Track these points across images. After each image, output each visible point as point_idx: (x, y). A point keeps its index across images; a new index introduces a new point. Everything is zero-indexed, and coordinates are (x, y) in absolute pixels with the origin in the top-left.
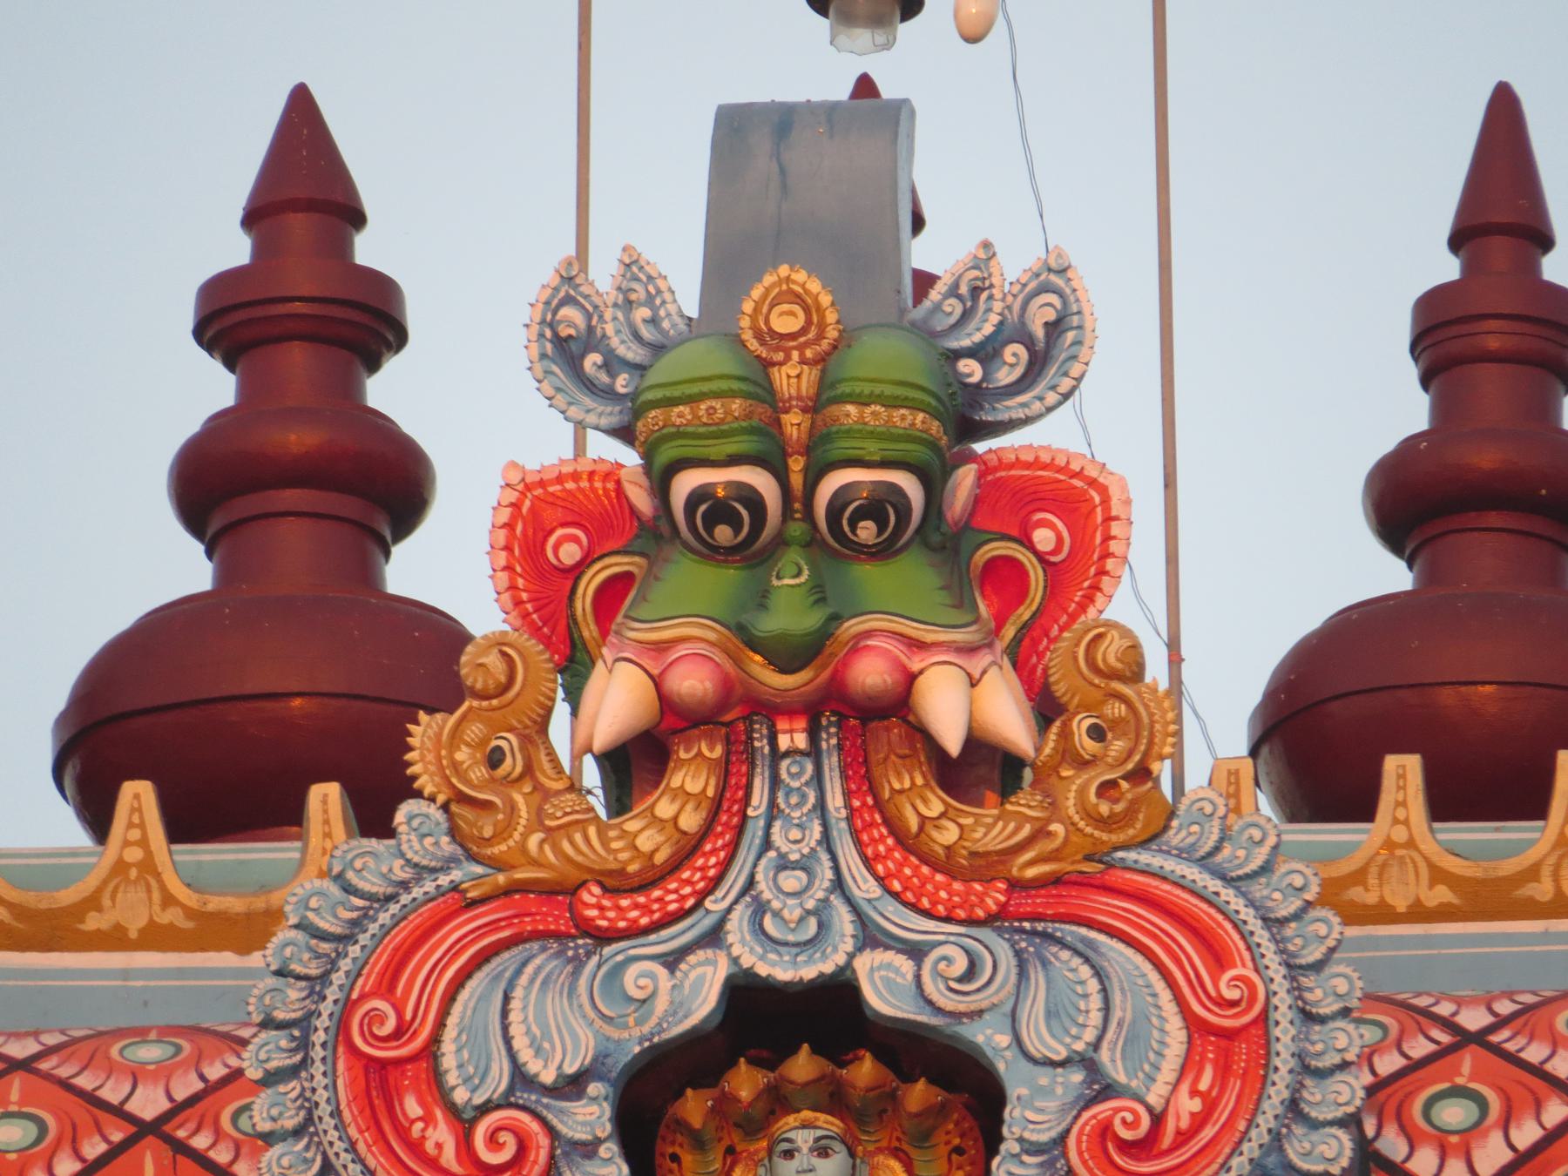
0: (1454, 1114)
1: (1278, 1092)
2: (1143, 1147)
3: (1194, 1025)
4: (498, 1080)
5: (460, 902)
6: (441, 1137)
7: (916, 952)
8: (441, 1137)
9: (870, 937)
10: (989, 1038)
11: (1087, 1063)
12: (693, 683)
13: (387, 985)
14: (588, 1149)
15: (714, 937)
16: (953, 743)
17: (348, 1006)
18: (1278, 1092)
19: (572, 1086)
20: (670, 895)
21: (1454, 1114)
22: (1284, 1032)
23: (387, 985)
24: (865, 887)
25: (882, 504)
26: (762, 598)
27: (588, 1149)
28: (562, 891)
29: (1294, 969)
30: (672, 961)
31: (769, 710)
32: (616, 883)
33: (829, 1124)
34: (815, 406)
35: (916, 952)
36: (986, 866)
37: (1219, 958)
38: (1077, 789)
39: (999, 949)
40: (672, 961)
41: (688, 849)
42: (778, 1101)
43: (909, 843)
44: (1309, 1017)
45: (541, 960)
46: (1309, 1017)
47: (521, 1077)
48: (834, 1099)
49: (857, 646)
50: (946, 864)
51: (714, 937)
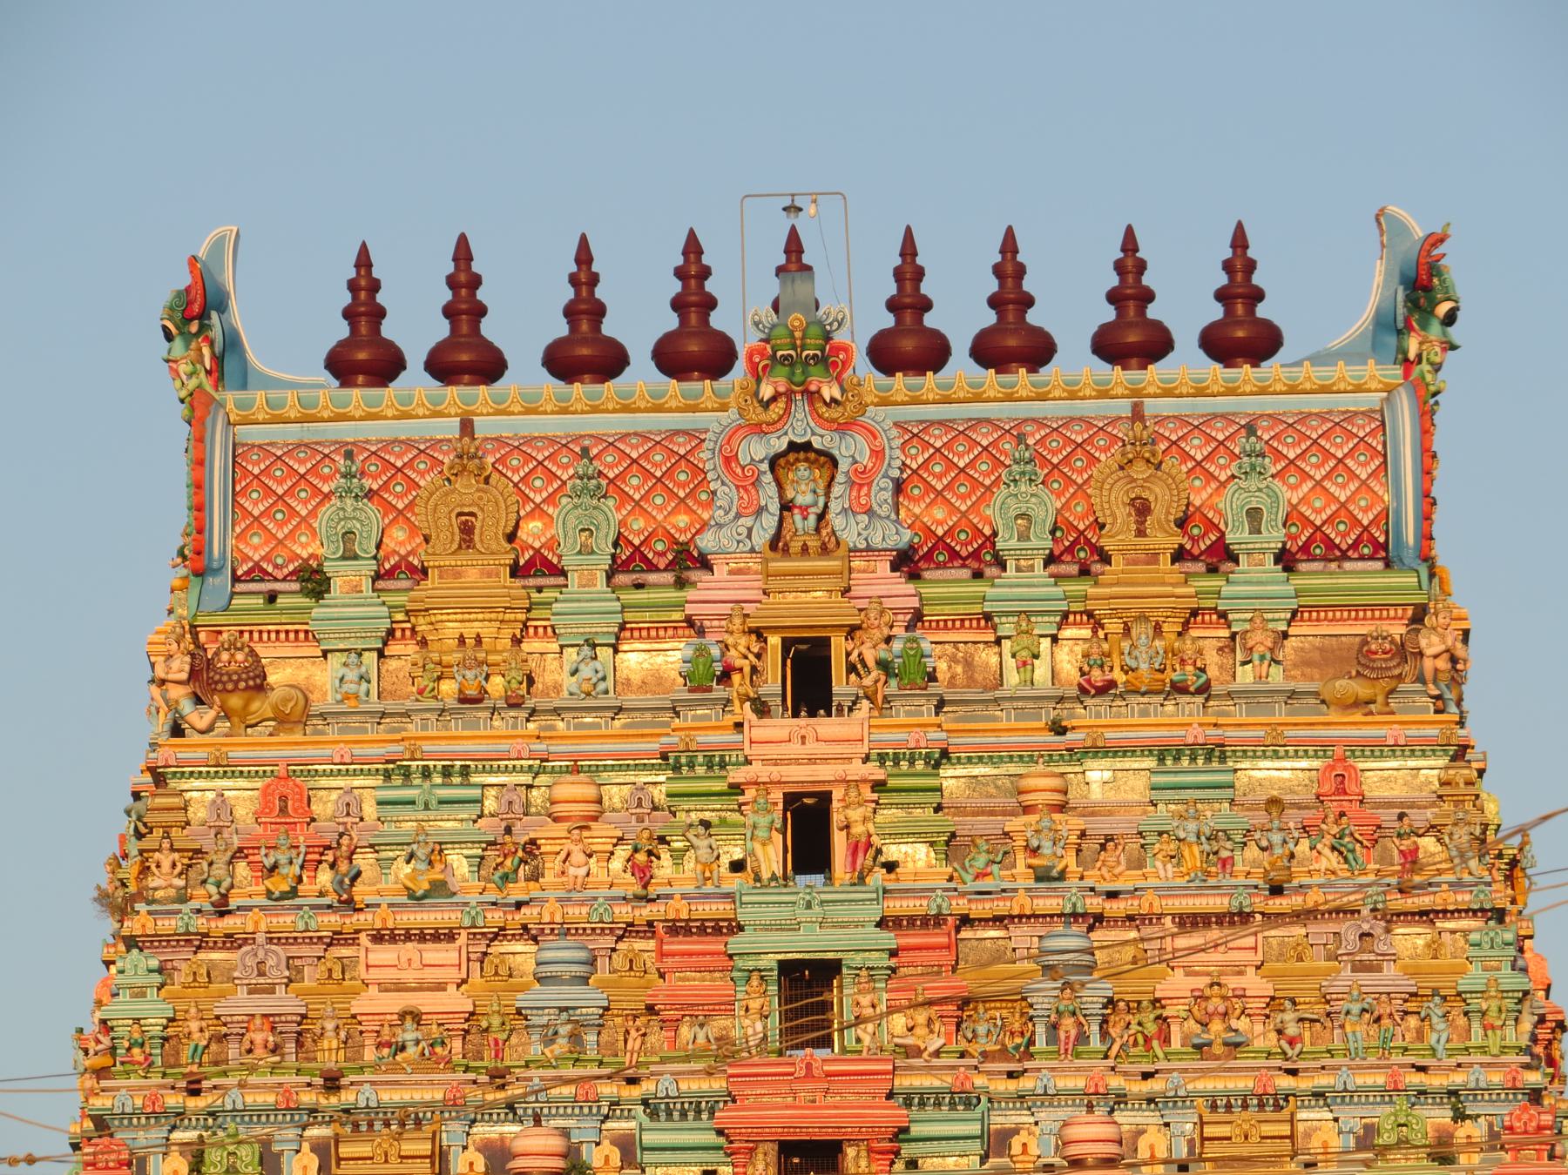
0: (913, 451)
1: (886, 462)
2: (862, 473)
3: (872, 450)
4: (749, 460)
5: (740, 427)
6: (739, 471)
7: (822, 436)
8: (739, 471)
9: (813, 434)
10: (835, 452)
11: (853, 457)
12: (782, 389)
13: (728, 443)
14: (765, 473)
15: (786, 433)
16: (828, 400)
17: (721, 447)
18: (886, 462)
19: (761, 461)
20: (778, 426)
21: (913, 451)
22: (887, 451)
23: (728, 443)
24: (812, 424)
25: (815, 356)
26: (793, 374)
27: (765, 473)
28: (759, 425)
29: (889, 440)
30: (779, 438)
31: (795, 392)
32: (768, 424)
33: (806, 465)
34: (803, 338)
35: (822, 436)
36: (834, 421)
37: (875, 437)
38: (849, 406)
39: (836, 436)
40: (779, 438)
41: (780, 418)
42: (797, 460)
43: (820, 416)
44: (891, 448)
45: (756, 438)
46: (891, 448)
47: (752, 459)
48: (807, 460)
49: (810, 383)
50: (826, 420)
51: (786, 433)
